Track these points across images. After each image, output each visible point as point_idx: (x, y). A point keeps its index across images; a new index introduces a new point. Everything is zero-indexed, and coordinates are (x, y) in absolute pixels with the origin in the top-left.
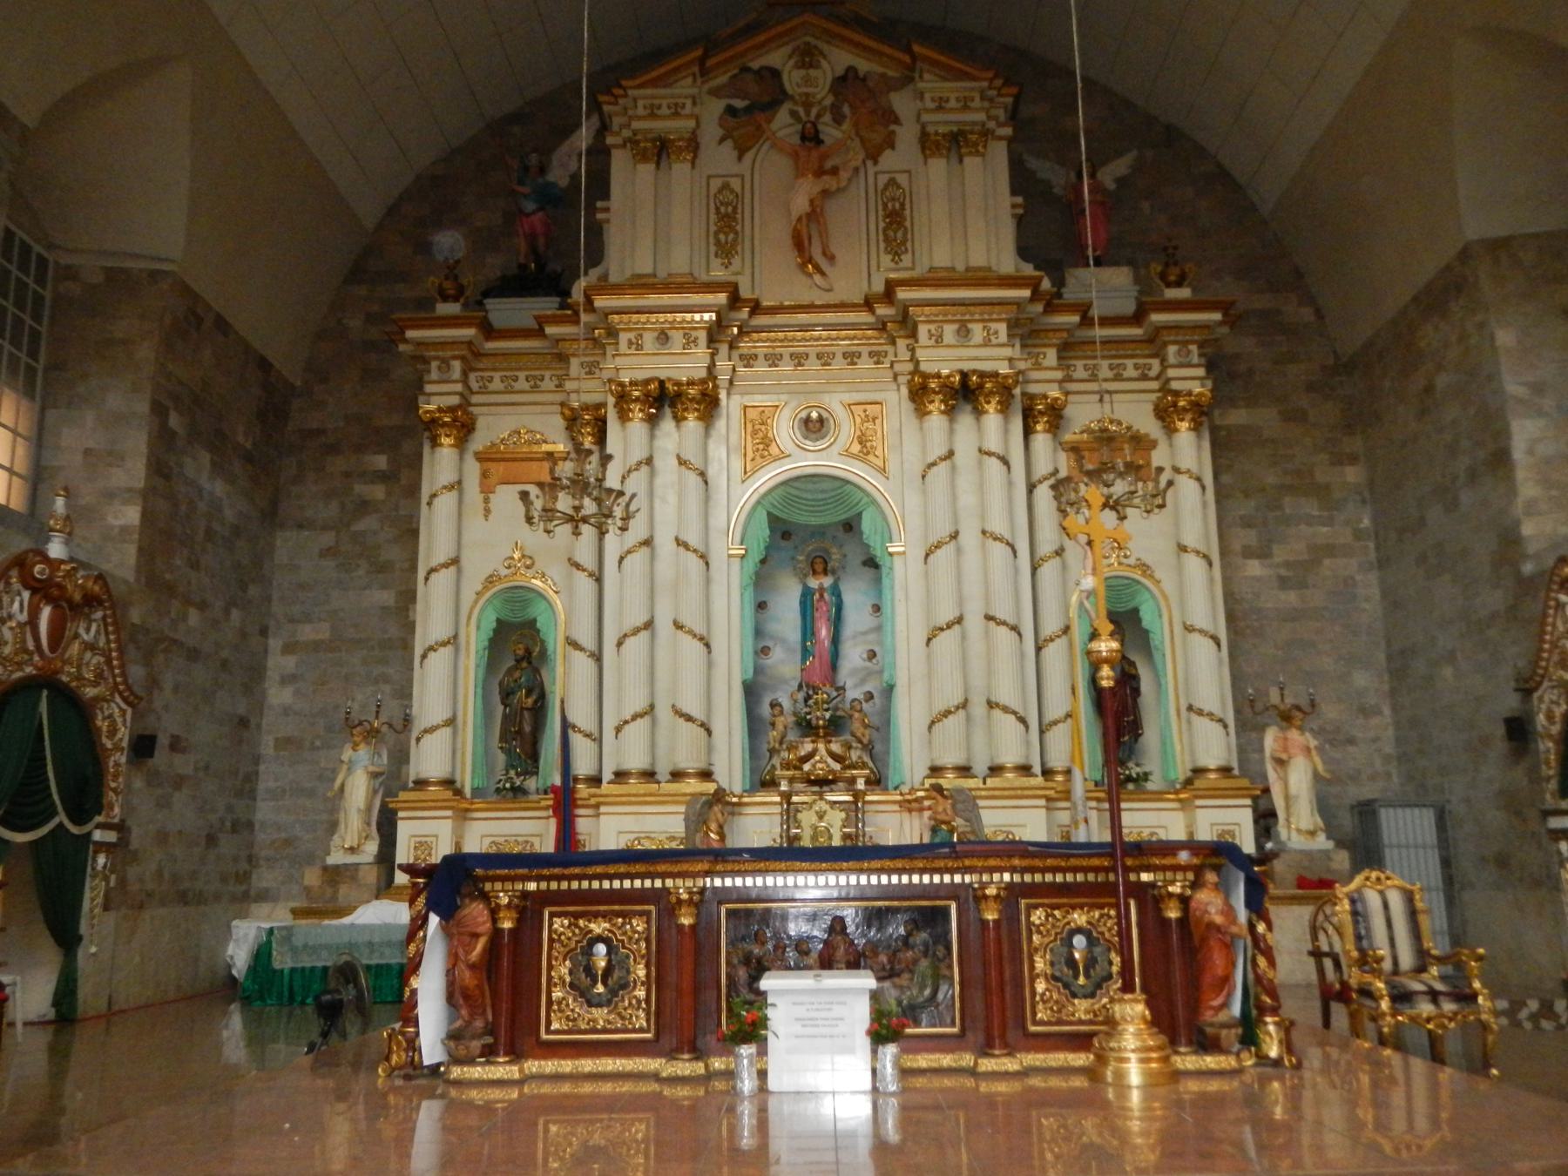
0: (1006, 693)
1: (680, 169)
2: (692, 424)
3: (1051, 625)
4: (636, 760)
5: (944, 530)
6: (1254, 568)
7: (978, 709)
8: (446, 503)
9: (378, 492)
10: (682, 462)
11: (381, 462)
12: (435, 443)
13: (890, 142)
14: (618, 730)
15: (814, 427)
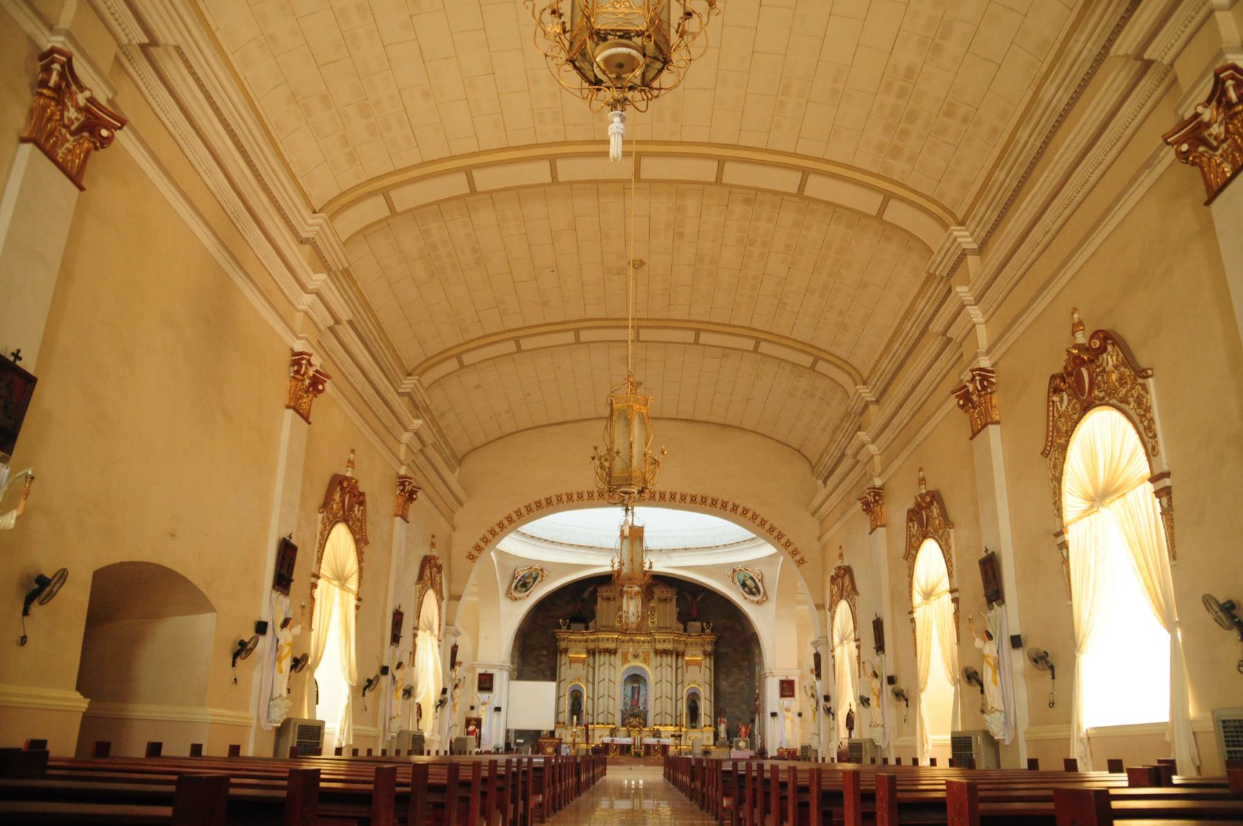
0: (669, 712)
1: (612, 603)
2: (613, 657)
3: (679, 697)
4: (601, 721)
5: (659, 679)
6: (724, 683)
7: (664, 713)
8: (563, 668)
9: (544, 659)
10: (610, 664)
11: (545, 653)
12: (561, 655)
13: (653, 598)
14: (598, 715)
15: (636, 656)
